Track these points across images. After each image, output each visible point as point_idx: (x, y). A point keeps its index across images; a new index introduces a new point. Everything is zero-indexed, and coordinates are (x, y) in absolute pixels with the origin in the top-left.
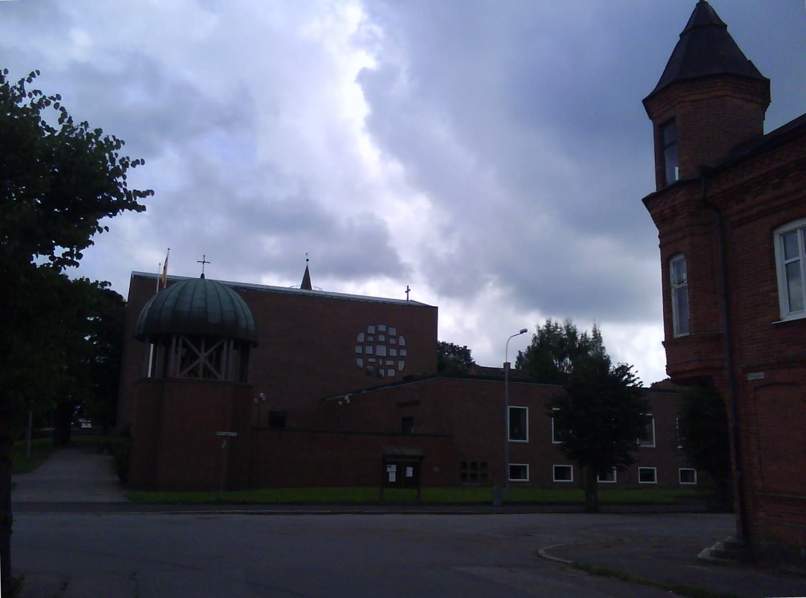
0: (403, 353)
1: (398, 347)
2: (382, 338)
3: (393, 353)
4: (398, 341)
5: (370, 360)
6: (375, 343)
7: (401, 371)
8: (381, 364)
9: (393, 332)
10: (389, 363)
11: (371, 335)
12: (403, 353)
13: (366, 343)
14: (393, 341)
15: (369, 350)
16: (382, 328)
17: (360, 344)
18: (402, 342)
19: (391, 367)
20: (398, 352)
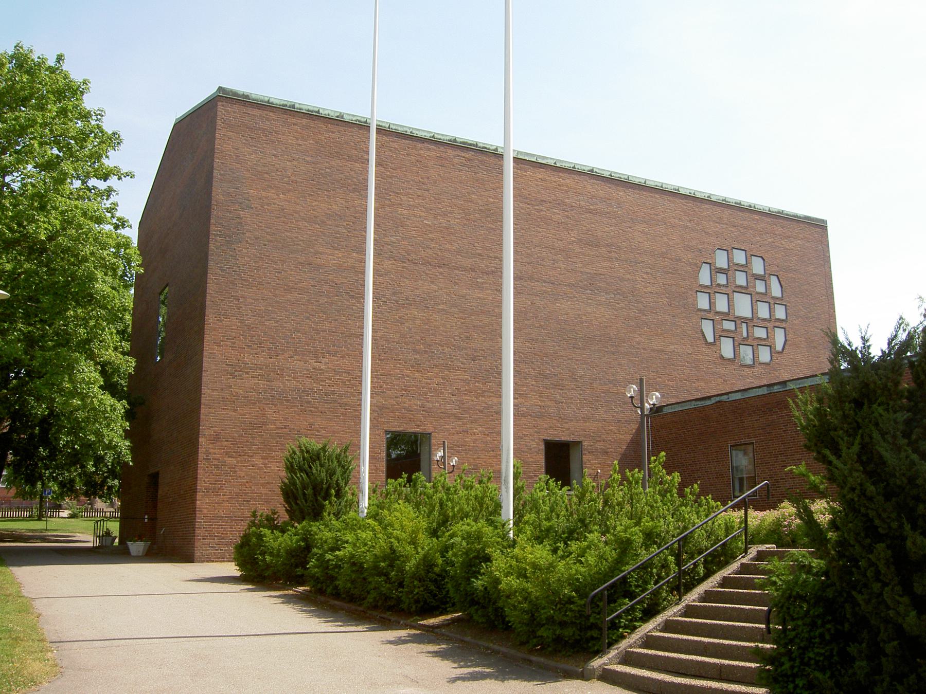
0: (780, 313)
1: (772, 302)
2: (741, 279)
3: (763, 311)
4: (767, 287)
5: (729, 326)
6: (732, 290)
7: (778, 352)
8: (745, 335)
9: (758, 267)
10: (760, 333)
11: (721, 271)
12: (780, 313)
13: (712, 290)
14: (760, 287)
15: (722, 304)
16: (739, 257)
17: (703, 289)
18: (776, 291)
19: (761, 342)
20: (771, 310)
